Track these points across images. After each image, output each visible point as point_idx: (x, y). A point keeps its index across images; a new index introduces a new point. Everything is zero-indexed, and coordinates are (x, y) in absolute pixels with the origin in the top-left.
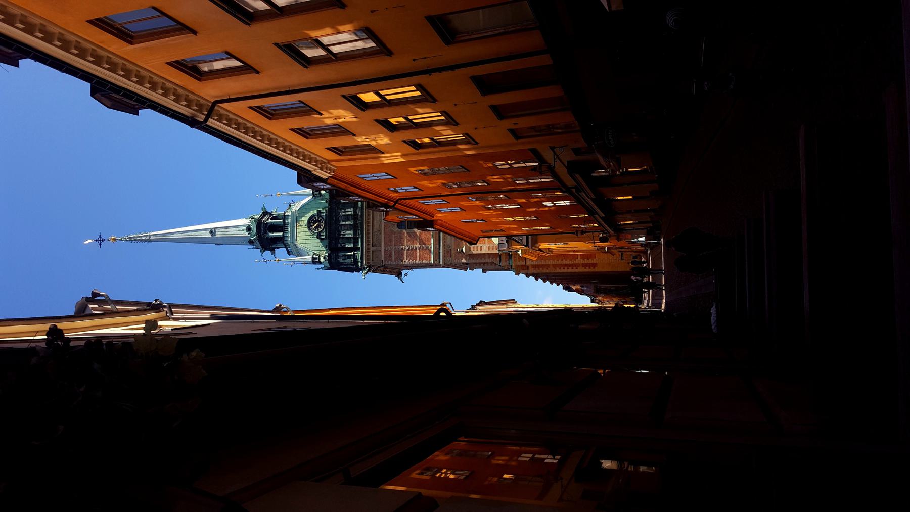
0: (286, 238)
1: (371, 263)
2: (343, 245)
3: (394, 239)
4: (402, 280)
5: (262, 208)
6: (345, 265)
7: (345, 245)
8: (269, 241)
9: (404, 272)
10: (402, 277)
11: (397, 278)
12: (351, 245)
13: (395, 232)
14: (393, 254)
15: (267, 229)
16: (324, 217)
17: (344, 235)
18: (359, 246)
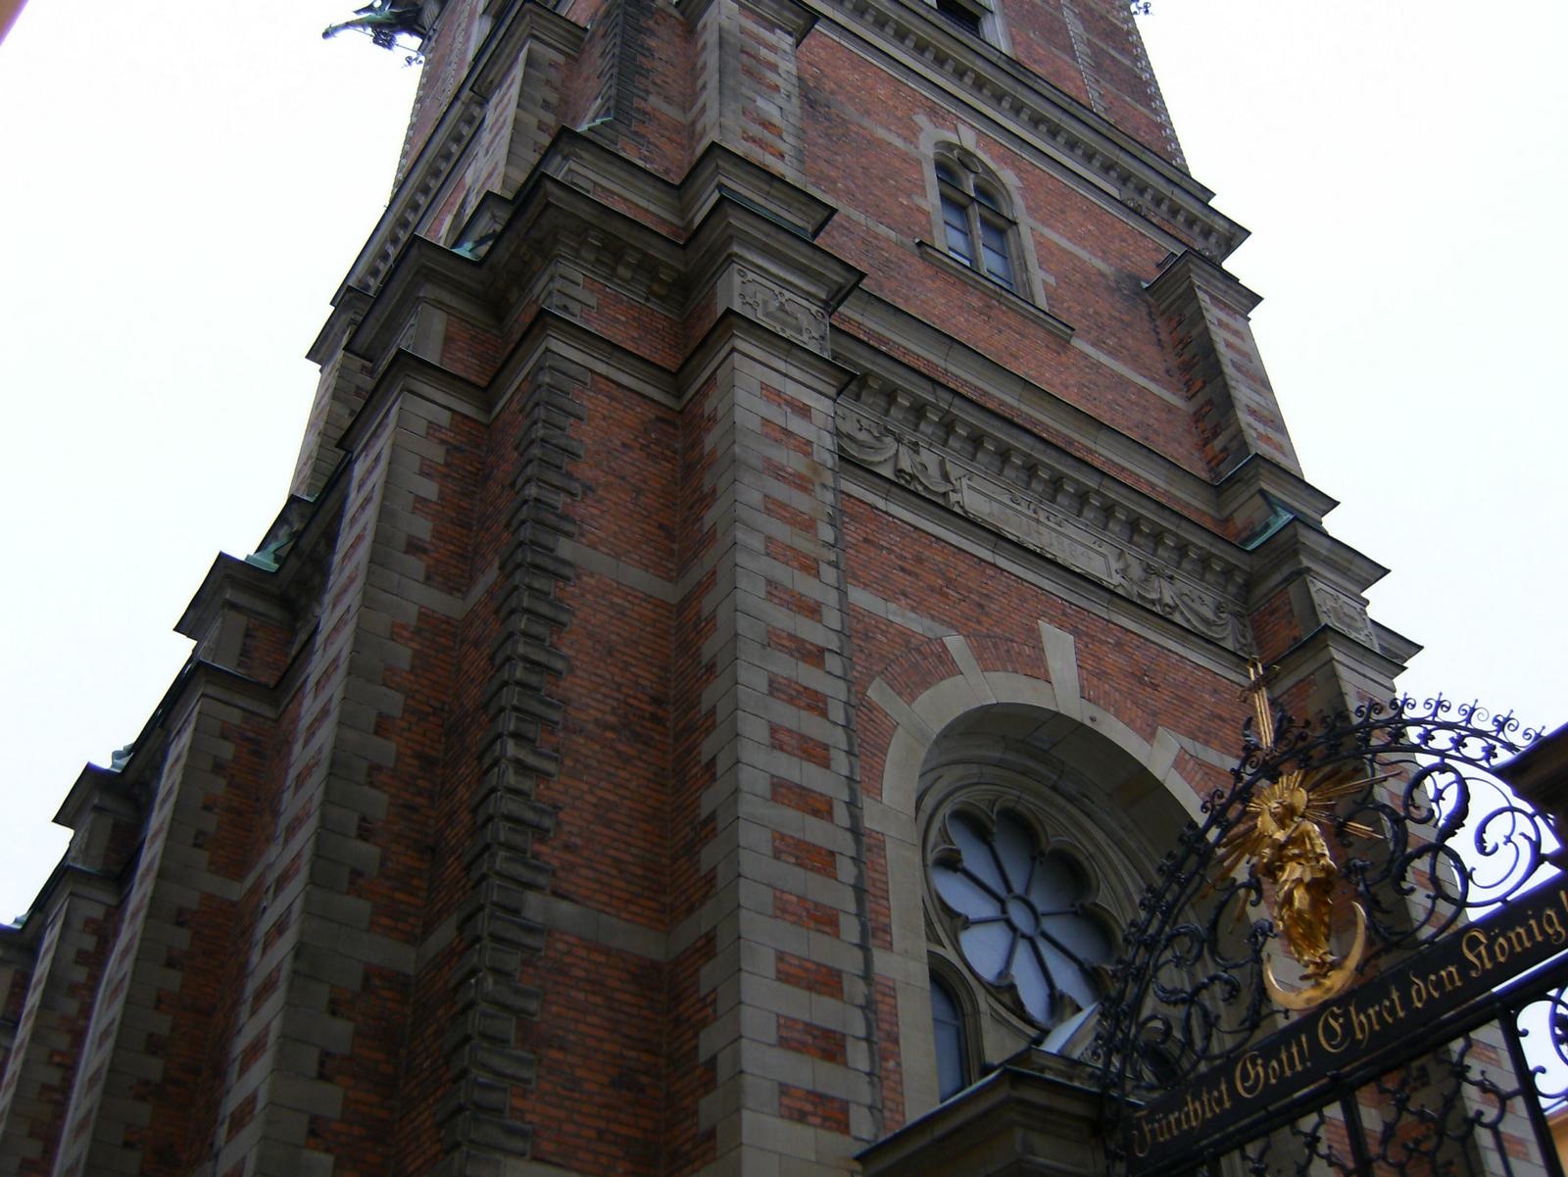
4: (347, 25)
9: (408, 42)
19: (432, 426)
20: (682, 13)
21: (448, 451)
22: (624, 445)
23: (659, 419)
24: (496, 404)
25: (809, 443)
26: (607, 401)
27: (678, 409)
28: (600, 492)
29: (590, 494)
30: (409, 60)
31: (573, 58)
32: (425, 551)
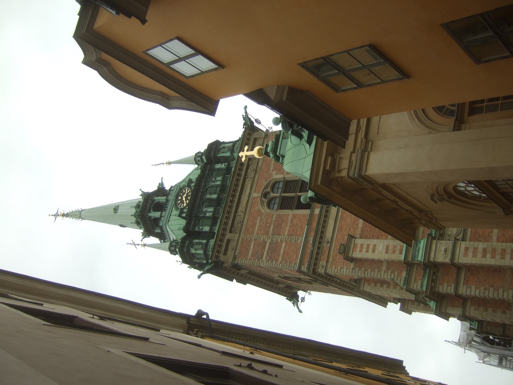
0: (163, 218)
1: (222, 258)
2: (201, 227)
3: (258, 222)
4: (298, 308)
5: (160, 183)
6: (198, 259)
7: (203, 228)
8: (152, 223)
9: (301, 294)
10: (299, 303)
11: (289, 303)
12: (207, 229)
13: (263, 213)
14: (252, 247)
15: (152, 206)
16: (193, 188)
17: (206, 212)
18: (216, 231)
19: (475, 310)
20: (353, 261)
21: (480, 306)
22: (478, 279)
23: (469, 271)
24: (466, 298)
25: (474, 248)
26: (469, 282)
27: (465, 268)
28: (491, 284)
29: (492, 286)
30: (310, 294)
31: (365, 280)
32: (504, 311)
